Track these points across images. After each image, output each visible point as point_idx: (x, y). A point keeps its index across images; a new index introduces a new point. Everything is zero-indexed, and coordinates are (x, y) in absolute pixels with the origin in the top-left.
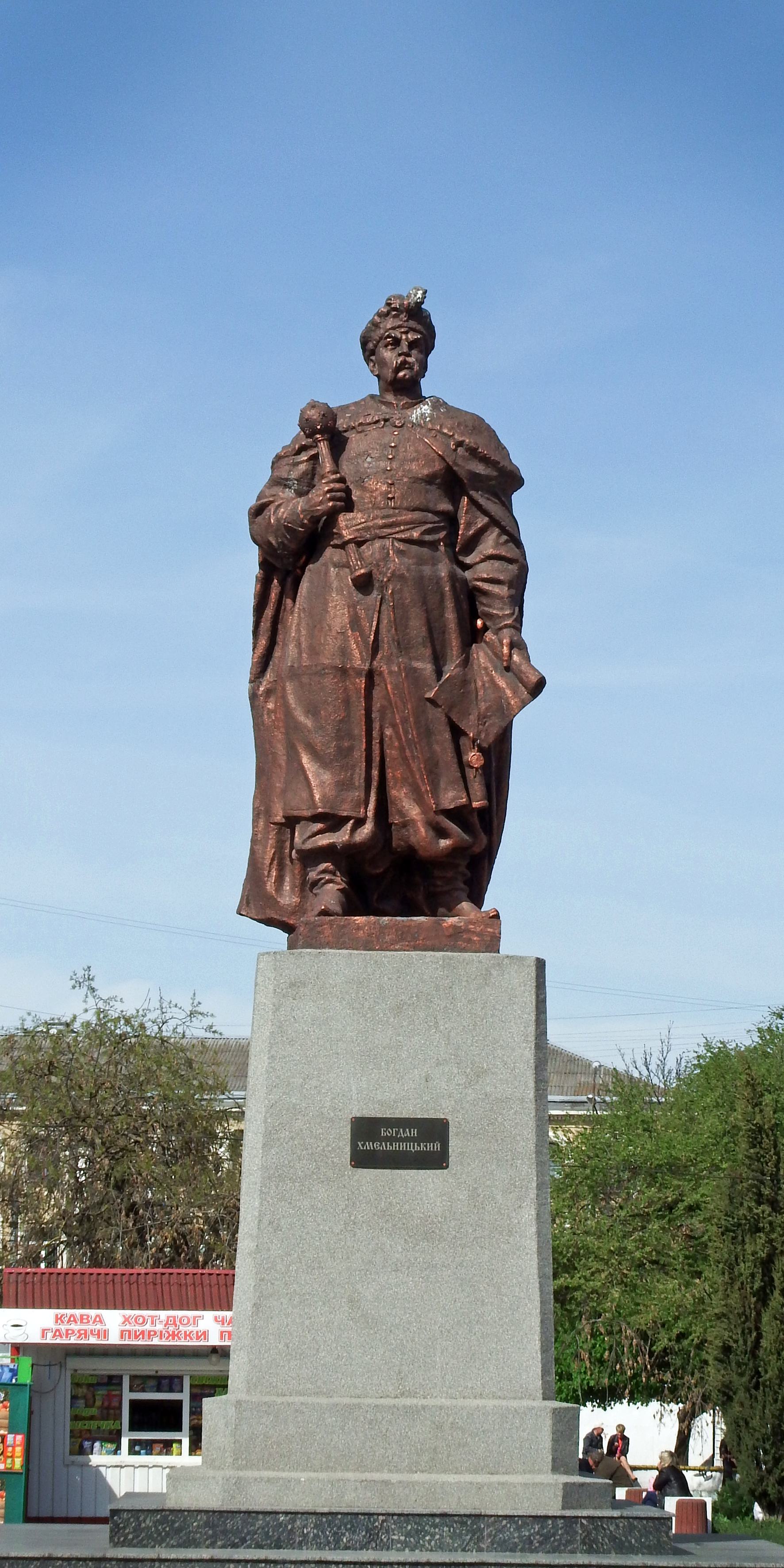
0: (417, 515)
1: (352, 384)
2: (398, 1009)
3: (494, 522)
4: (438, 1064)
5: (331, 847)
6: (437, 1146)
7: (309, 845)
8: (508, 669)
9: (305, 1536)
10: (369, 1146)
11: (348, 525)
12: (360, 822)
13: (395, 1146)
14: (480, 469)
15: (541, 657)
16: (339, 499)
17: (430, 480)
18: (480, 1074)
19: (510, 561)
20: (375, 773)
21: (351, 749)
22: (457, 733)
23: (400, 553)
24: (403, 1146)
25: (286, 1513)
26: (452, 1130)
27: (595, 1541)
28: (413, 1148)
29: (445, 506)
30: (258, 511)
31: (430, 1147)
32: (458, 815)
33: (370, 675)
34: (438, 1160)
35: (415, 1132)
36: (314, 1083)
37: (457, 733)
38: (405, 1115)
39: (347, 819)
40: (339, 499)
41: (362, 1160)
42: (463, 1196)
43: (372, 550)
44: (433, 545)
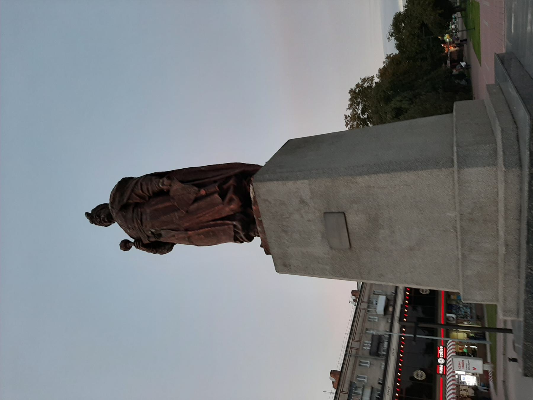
0: (135, 220)
2: (285, 232)
4: (302, 217)
5: (245, 235)
12: (235, 226)
14: (117, 199)
16: (139, 244)
17: (124, 217)
18: (302, 202)
19: (141, 185)
20: (219, 222)
21: (213, 232)
22: (196, 200)
26: (328, 211)
29: (131, 209)
32: (223, 196)
33: (187, 230)
37: (196, 200)
40: (139, 244)
42: (355, 206)
44: (141, 214)
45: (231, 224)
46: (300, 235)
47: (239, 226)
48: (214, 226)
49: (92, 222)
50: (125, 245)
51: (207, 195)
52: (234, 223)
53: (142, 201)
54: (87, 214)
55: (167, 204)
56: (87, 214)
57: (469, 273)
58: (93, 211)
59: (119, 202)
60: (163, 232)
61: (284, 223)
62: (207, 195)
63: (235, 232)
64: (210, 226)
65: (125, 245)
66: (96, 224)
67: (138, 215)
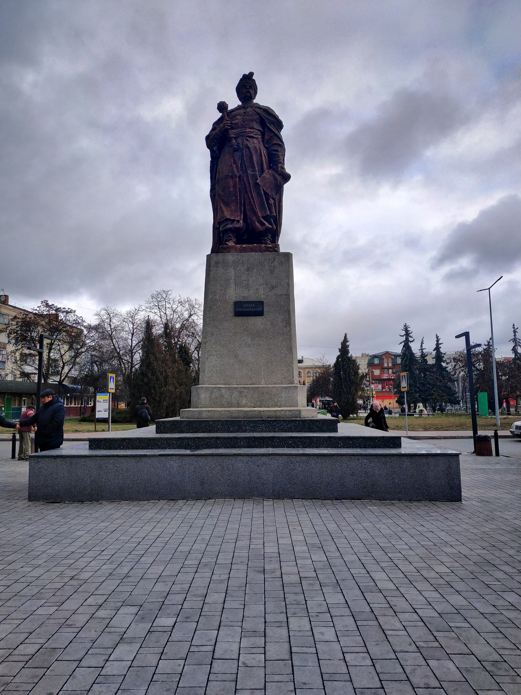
0: (252, 130)
1: (233, 102)
2: (248, 270)
3: (275, 135)
4: (260, 285)
5: (230, 228)
6: (261, 309)
7: (223, 229)
8: (279, 175)
9: (218, 428)
10: (240, 310)
11: (232, 133)
12: (238, 221)
13: (248, 310)
15: (288, 169)
18: (273, 288)
23: (247, 140)
24: (250, 310)
25: (212, 421)
27: (313, 428)
28: (253, 310)
30: (208, 138)
31: (258, 309)
34: (260, 314)
35: (254, 305)
36: (223, 292)
38: (251, 300)
39: (235, 220)
41: (238, 314)
43: (239, 140)
45: (240, 218)
46: (246, 280)
47: (237, 226)
48: (241, 203)
49: (245, 76)
50: (222, 107)
51: (268, 204)
52: (241, 222)
53: (266, 140)
54: (251, 74)
55: (265, 166)
56: (251, 74)
57: (223, 391)
58: (254, 81)
59: (269, 119)
60: (238, 154)
61: (255, 270)
62: (268, 204)
63: (233, 221)
64: (240, 199)
65: (222, 107)
66: (241, 80)
67: (255, 134)
